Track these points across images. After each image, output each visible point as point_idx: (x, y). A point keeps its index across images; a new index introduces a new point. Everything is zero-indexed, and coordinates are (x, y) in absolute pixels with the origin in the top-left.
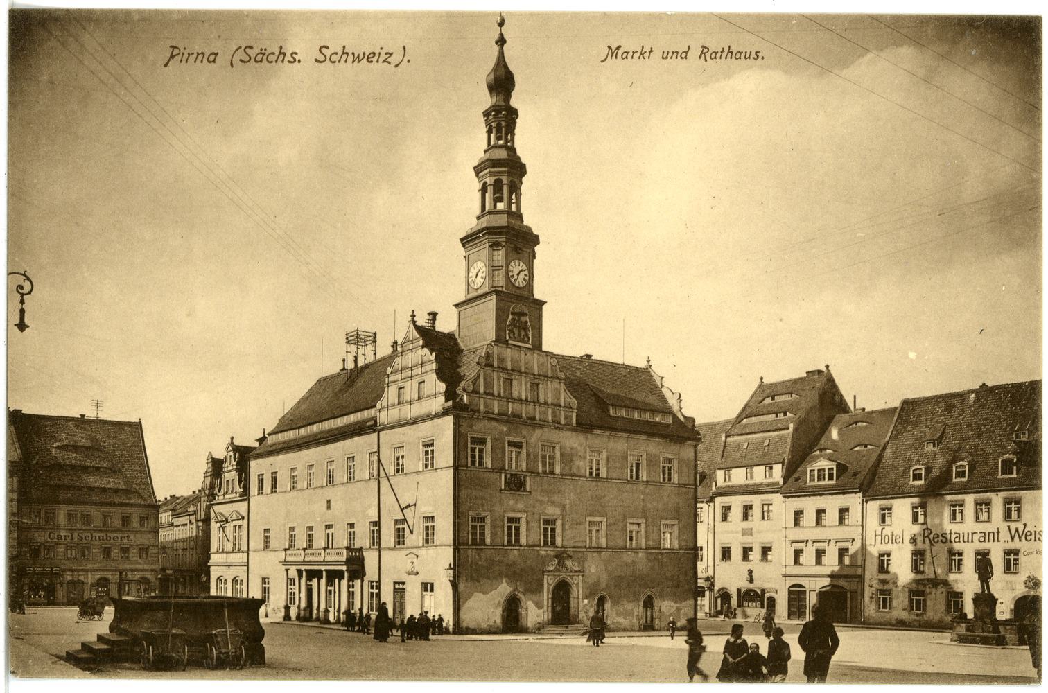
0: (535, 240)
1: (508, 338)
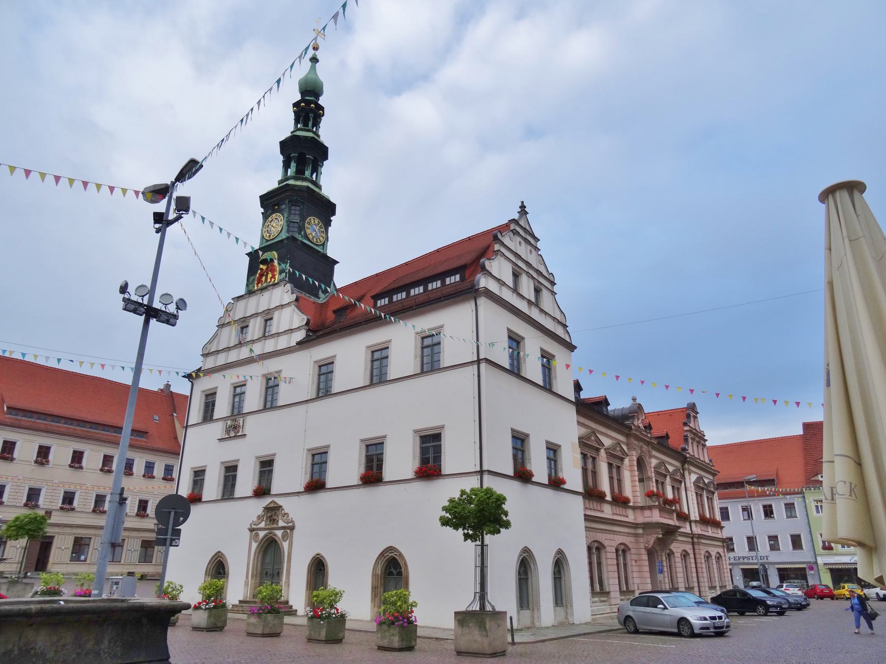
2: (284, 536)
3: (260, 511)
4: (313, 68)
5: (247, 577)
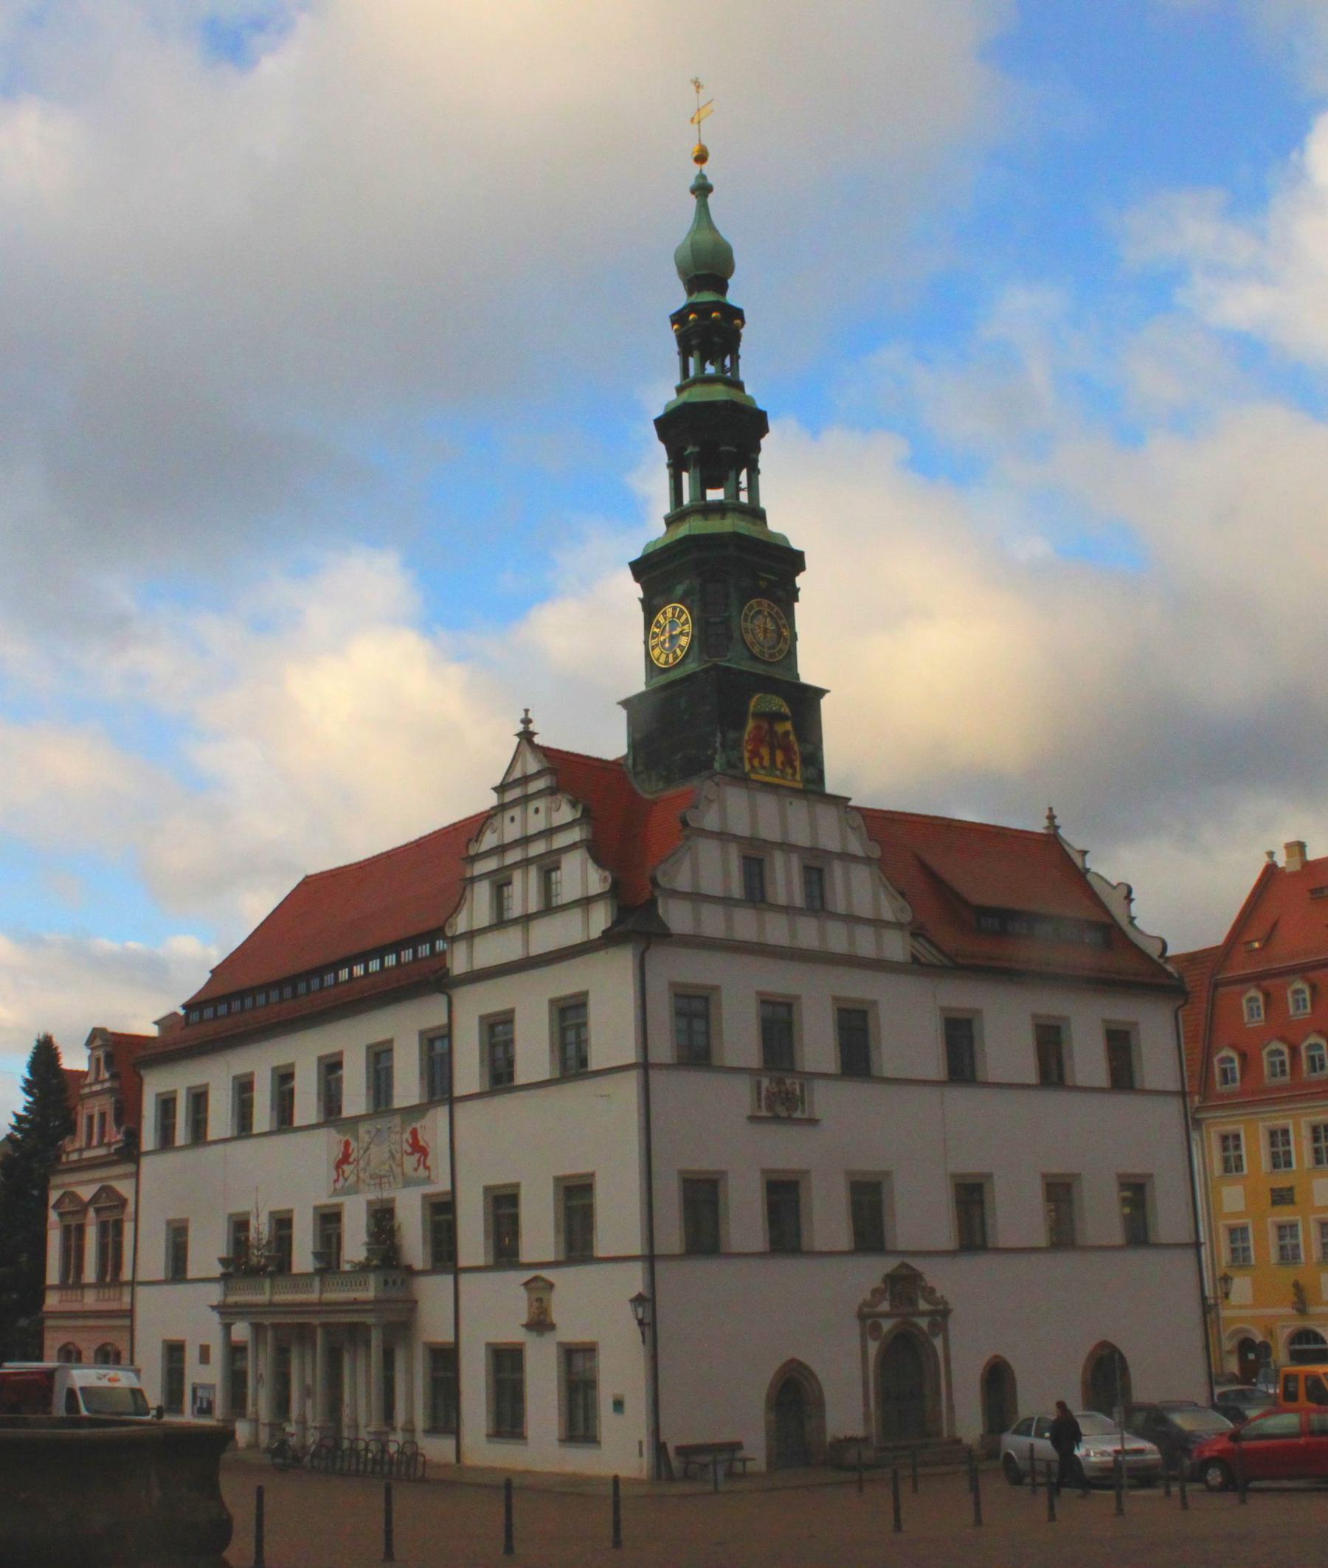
0: (795, 561)
1: (747, 767)
3: (878, 1283)
5: (866, 1405)
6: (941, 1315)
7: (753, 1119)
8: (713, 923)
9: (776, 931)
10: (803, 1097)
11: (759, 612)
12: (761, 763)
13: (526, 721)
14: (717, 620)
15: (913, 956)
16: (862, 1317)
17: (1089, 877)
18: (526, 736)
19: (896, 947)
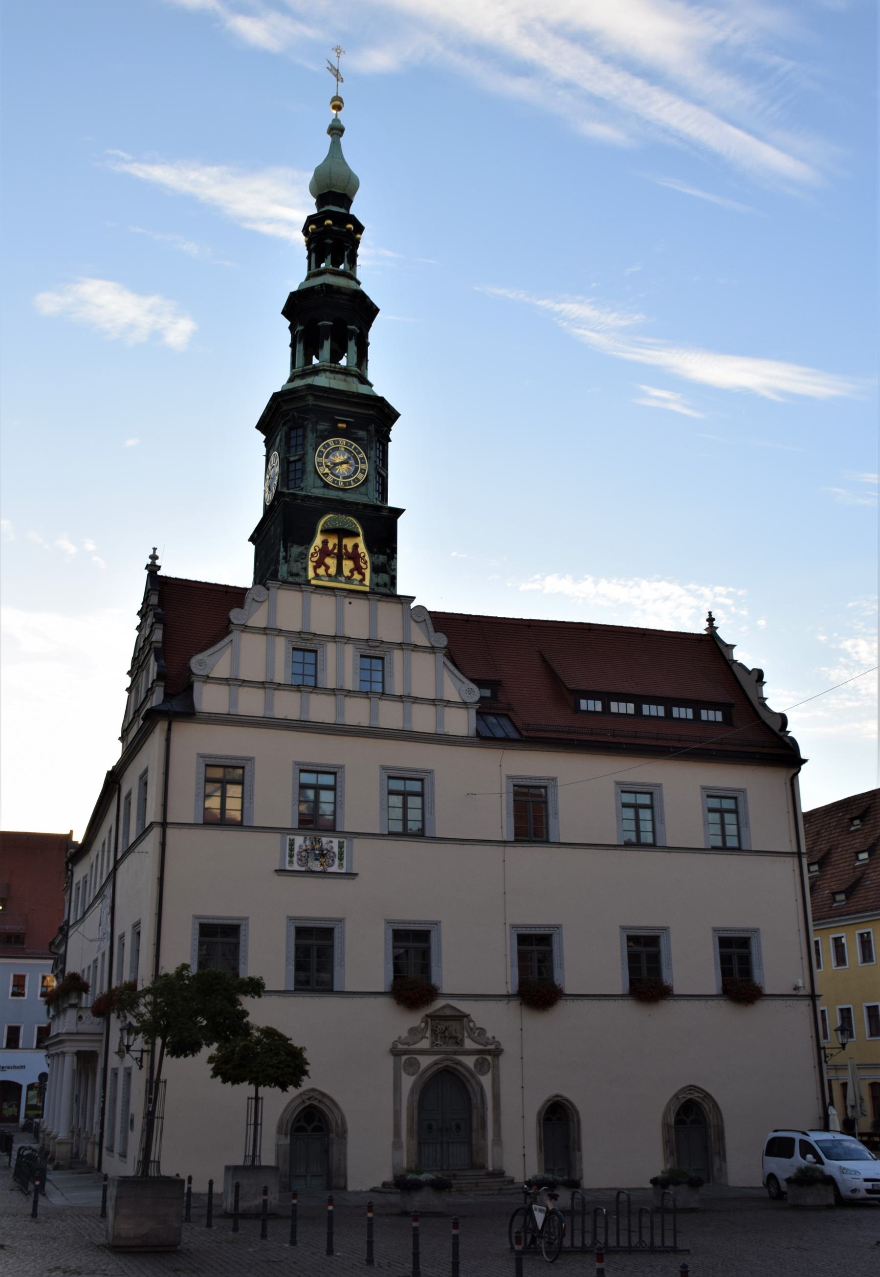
2: (482, 1066)
4: (336, 148)
6: (492, 1053)
7: (281, 872)
8: (251, 703)
9: (321, 709)
10: (341, 854)
11: (337, 449)
12: (326, 571)
13: (154, 557)
14: (296, 458)
15: (477, 731)
16: (396, 1053)
17: (734, 667)
18: (152, 568)
19: (461, 722)
